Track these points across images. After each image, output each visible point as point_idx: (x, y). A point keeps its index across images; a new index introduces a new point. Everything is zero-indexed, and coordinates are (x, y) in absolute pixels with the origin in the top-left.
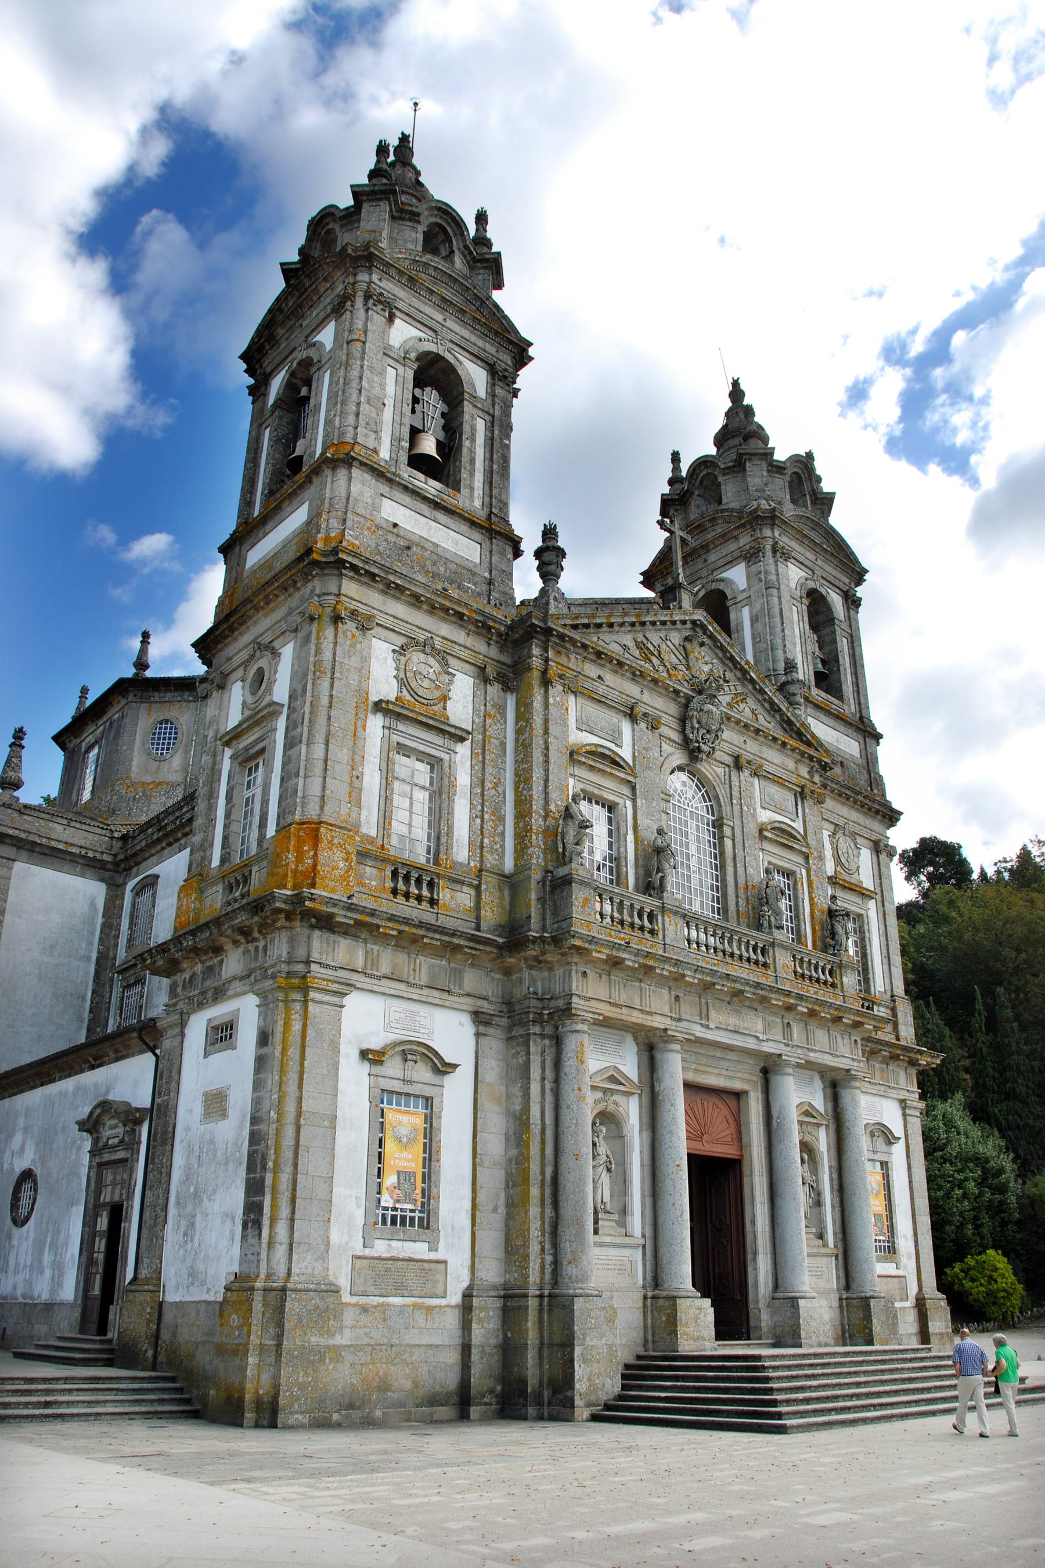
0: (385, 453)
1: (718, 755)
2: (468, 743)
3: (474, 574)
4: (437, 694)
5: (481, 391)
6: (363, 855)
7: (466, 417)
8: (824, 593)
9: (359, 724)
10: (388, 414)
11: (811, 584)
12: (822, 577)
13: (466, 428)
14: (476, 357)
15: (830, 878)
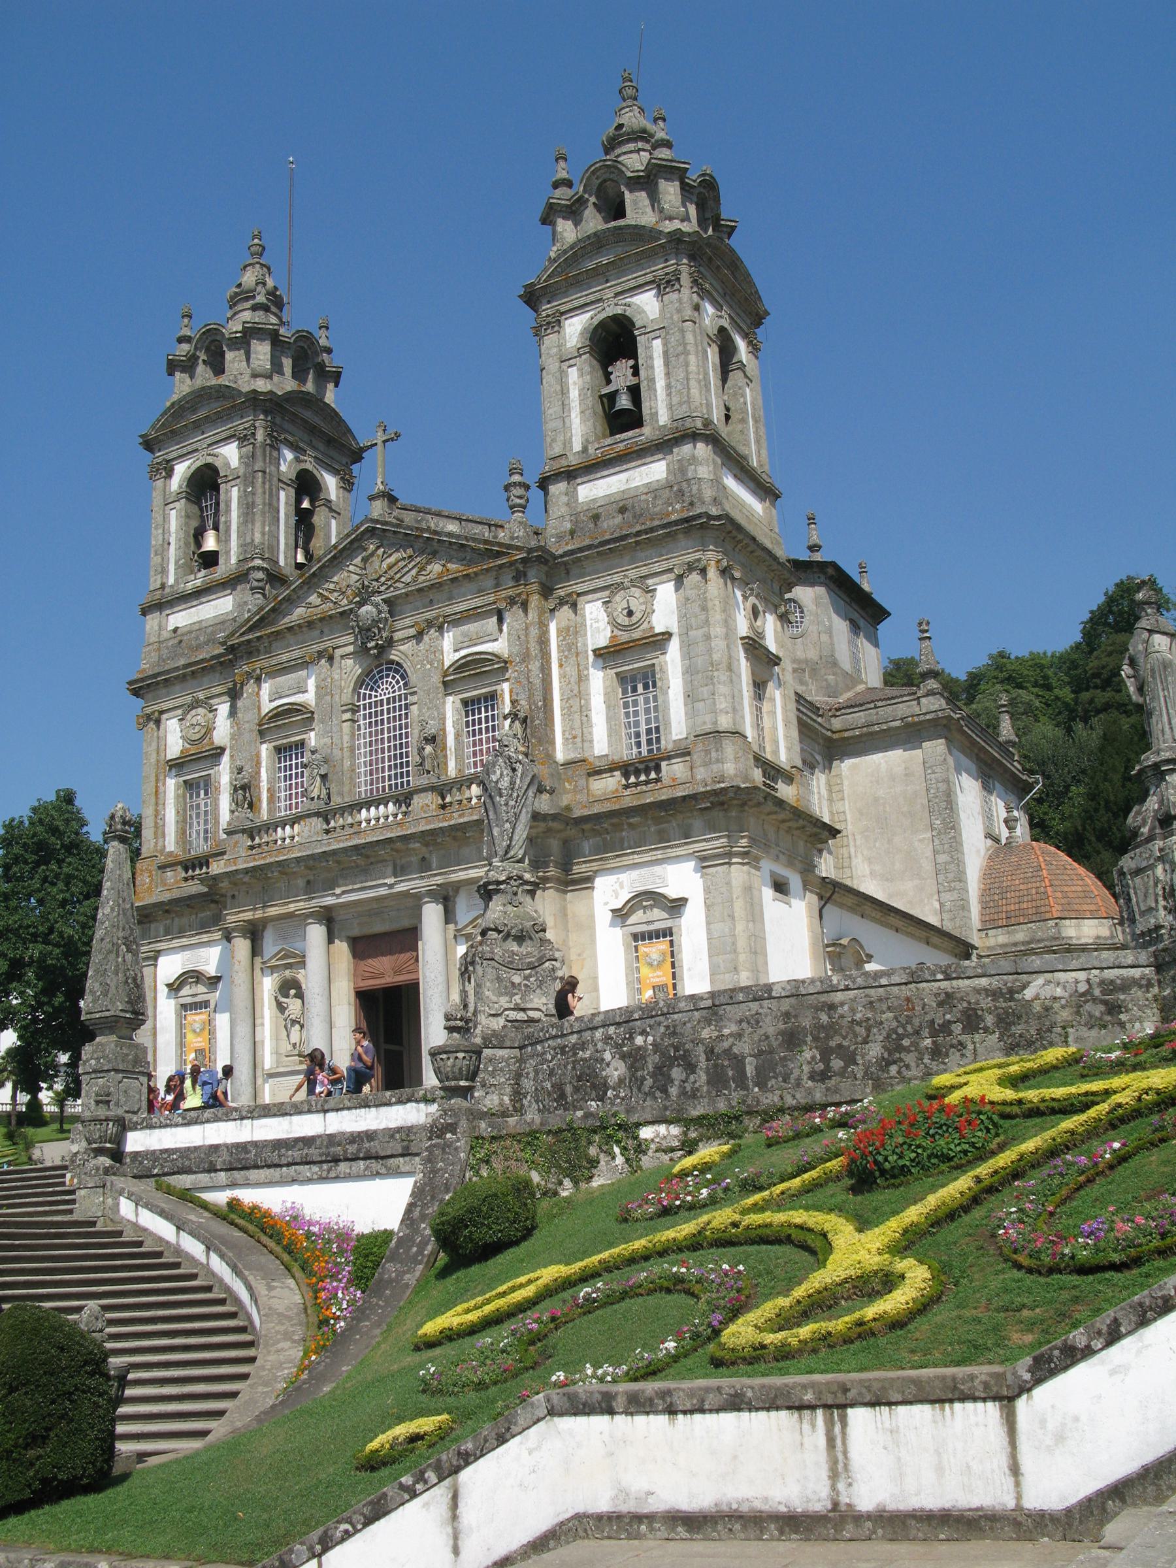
0: (171, 581)
1: (398, 636)
2: (227, 752)
3: (223, 623)
4: (203, 731)
5: (234, 462)
6: (163, 867)
7: (222, 497)
8: (619, 310)
9: (160, 784)
10: (172, 548)
11: (596, 322)
12: (617, 295)
13: (222, 505)
14: (226, 440)
15: (598, 653)
